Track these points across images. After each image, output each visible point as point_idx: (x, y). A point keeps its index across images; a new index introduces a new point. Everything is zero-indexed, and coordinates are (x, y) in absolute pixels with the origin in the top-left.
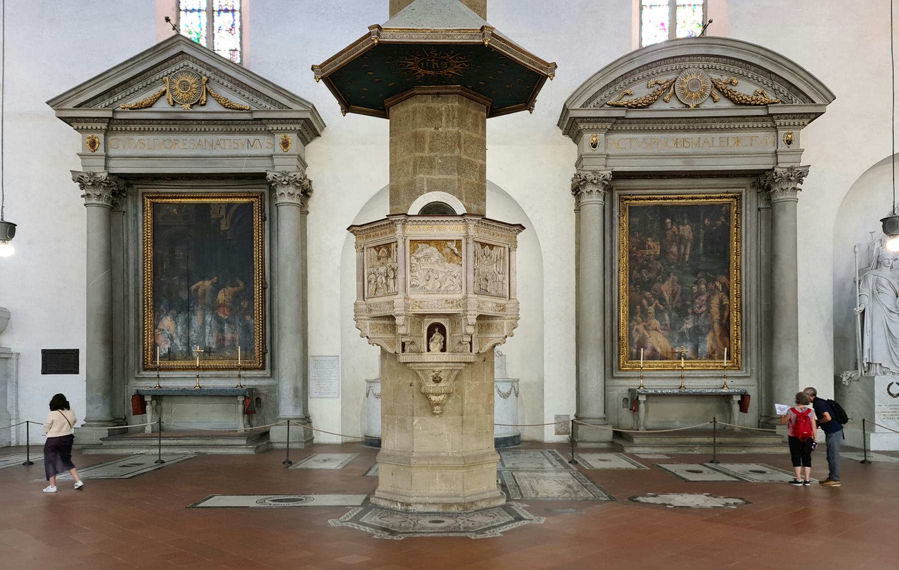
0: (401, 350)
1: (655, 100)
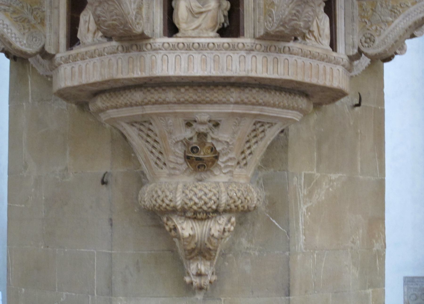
0: (63, 41)
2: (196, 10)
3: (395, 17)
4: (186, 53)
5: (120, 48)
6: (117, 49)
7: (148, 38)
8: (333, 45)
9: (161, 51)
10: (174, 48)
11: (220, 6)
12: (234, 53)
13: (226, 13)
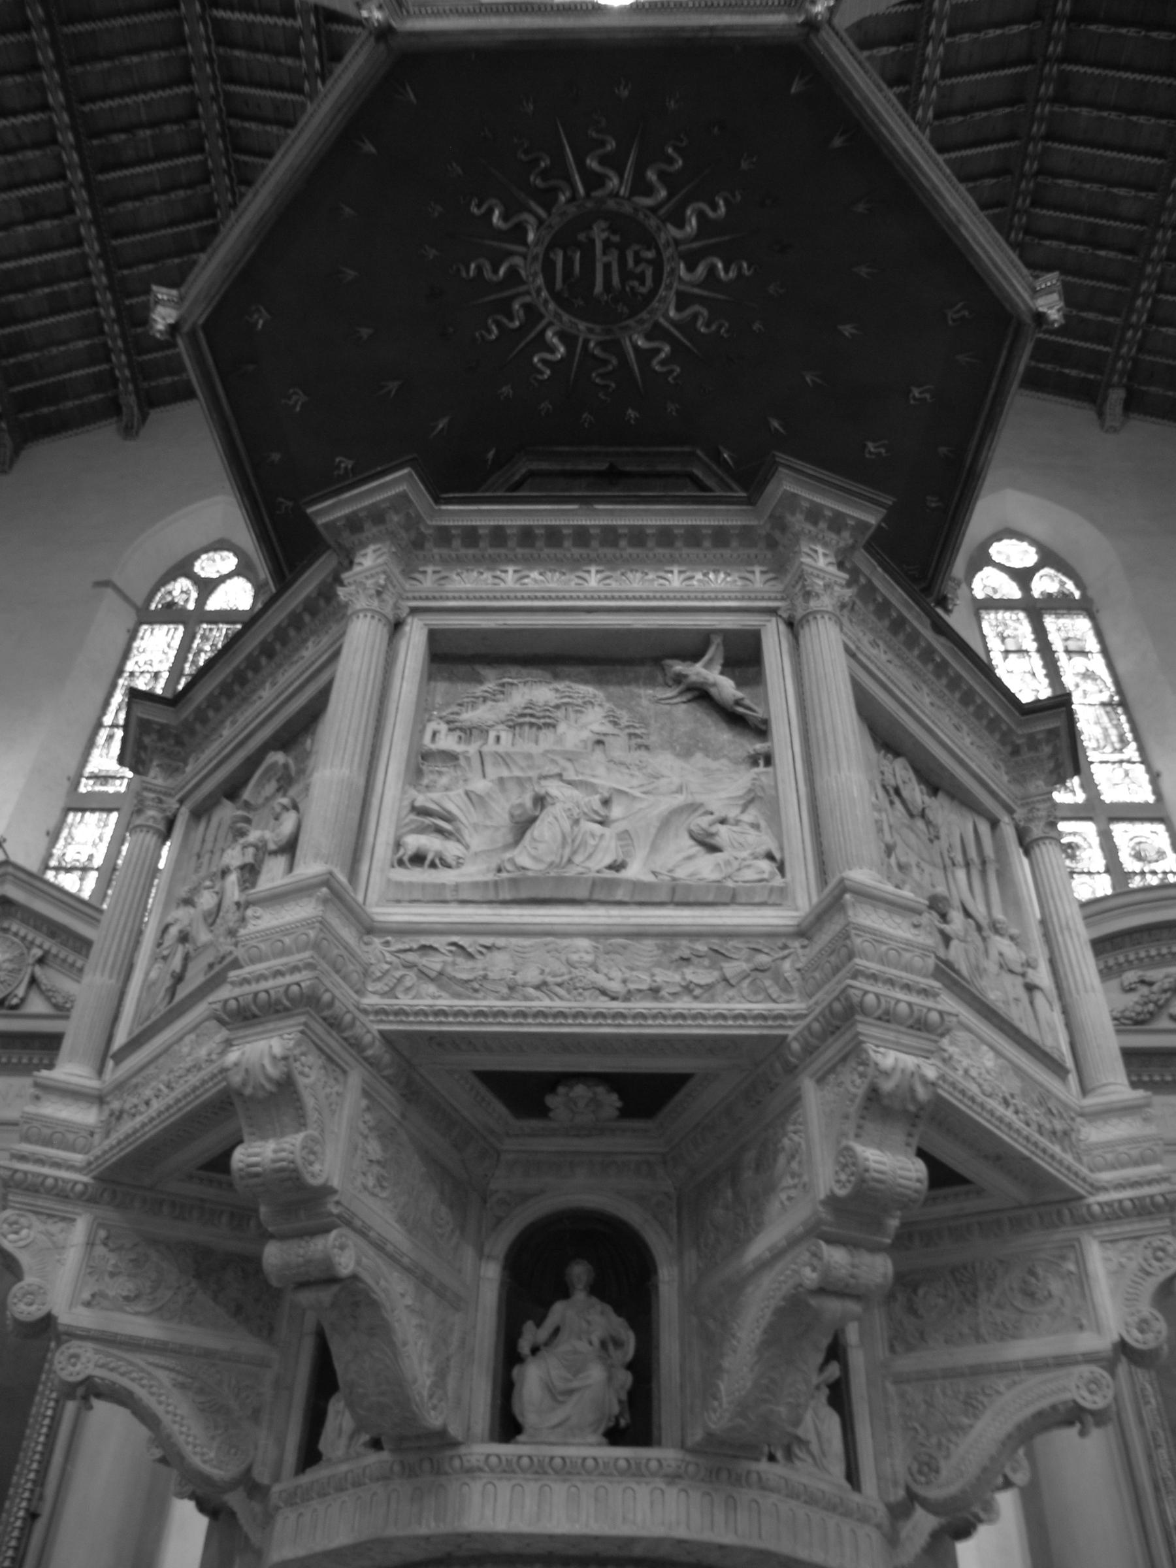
0: (291, 1456)
1: (1151, 1014)
2: (560, 1385)
3: (976, 1417)
4: (536, 1480)
5: (397, 1468)
6: (391, 1469)
7: (455, 1444)
8: (852, 1476)
9: (482, 1475)
10: (508, 1469)
11: (610, 1379)
12: (638, 1483)
13: (624, 1396)
